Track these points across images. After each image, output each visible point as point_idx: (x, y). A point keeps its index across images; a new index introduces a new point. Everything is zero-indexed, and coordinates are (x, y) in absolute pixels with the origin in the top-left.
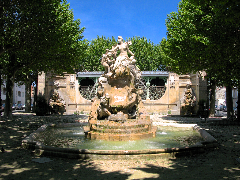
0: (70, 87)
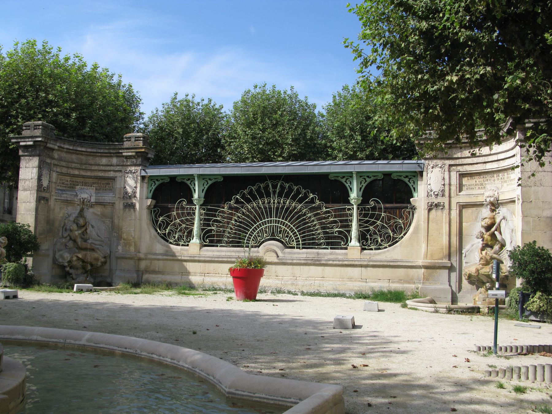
0: (121, 206)
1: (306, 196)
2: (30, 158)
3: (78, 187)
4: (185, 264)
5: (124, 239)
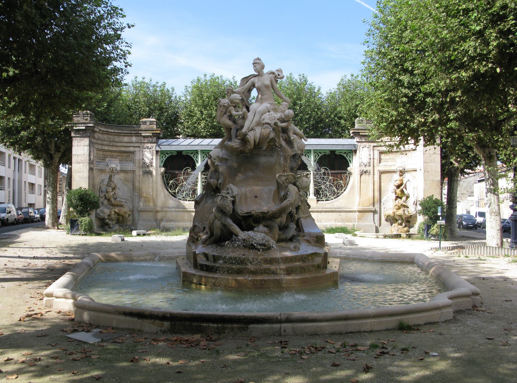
0: (141, 173)
3: (107, 159)
5: (144, 197)
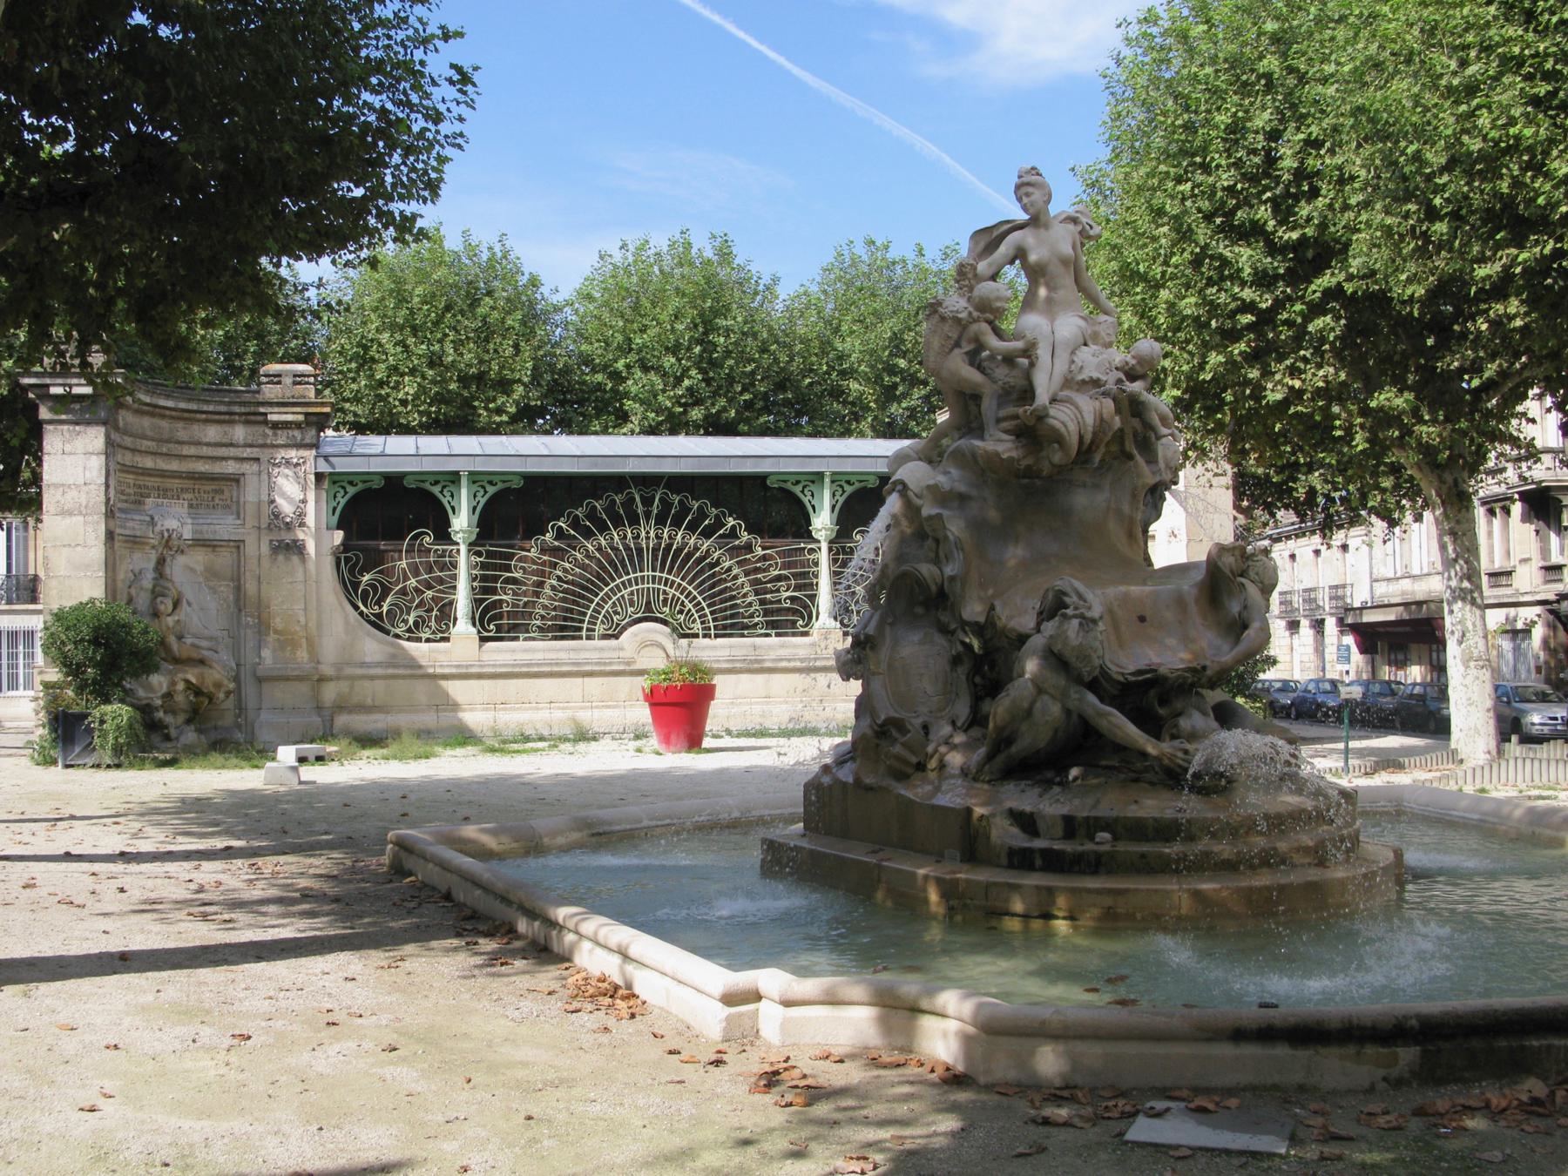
0: (265, 549)
1: (719, 524)
2: (77, 428)
3: (149, 501)
4: (444, 683)
5: (276, 632)
